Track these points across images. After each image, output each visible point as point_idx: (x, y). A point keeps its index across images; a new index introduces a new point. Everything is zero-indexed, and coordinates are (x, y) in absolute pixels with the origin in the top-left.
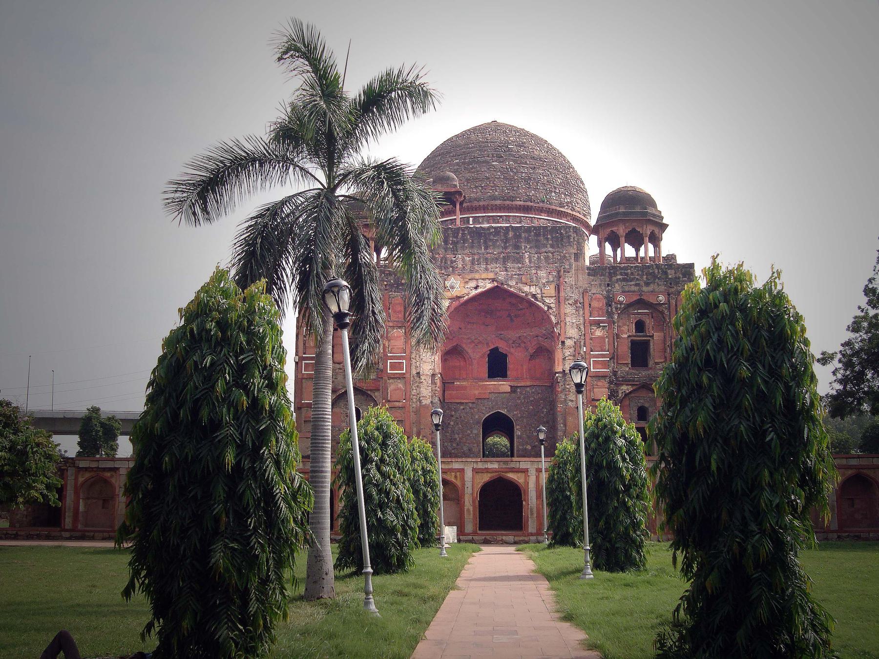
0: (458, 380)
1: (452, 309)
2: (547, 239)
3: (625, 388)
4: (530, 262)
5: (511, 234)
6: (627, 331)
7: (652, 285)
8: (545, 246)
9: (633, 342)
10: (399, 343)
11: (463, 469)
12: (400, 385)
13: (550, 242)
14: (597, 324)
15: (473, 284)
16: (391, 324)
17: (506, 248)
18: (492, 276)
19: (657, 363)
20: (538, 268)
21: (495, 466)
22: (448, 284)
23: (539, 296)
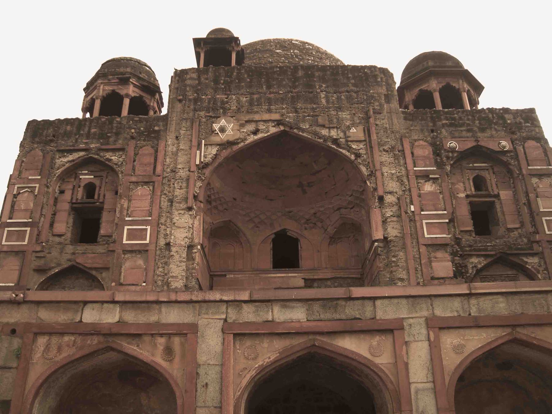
0: (231, 271)
1: (220, 160)
2: (348, 78)
3: (476, 262)
4: (328, 102)
5: (300, 73)
6: (463, 189)
7: (488, 131)
8: (346, 85)
9: (471, 203)
10: (145, 204)
11: (194, 328)
12: (140, 262)
13: (353, 81)
14: (425, 176)
15: (251, 127)
16: (134, 179)
17: (295, 87)
18: (276, 117)
19: (510, 230)
20: (340, 109)
21: (298, 315)
22: (216, 127)
23: (343, 140)
